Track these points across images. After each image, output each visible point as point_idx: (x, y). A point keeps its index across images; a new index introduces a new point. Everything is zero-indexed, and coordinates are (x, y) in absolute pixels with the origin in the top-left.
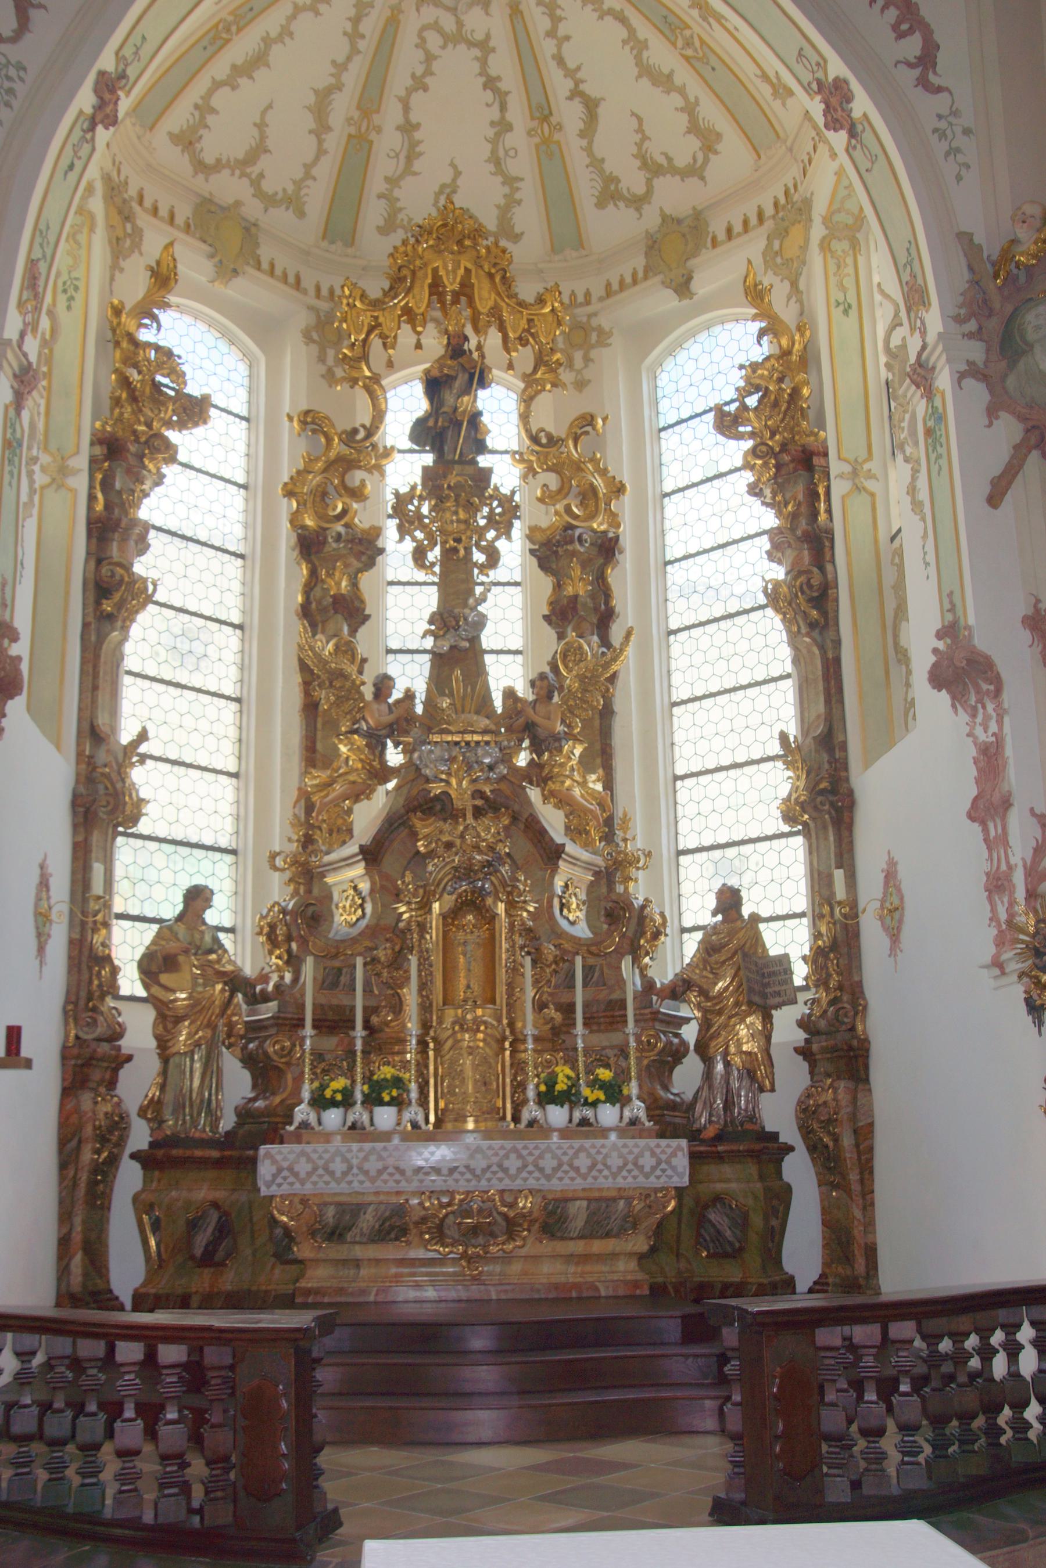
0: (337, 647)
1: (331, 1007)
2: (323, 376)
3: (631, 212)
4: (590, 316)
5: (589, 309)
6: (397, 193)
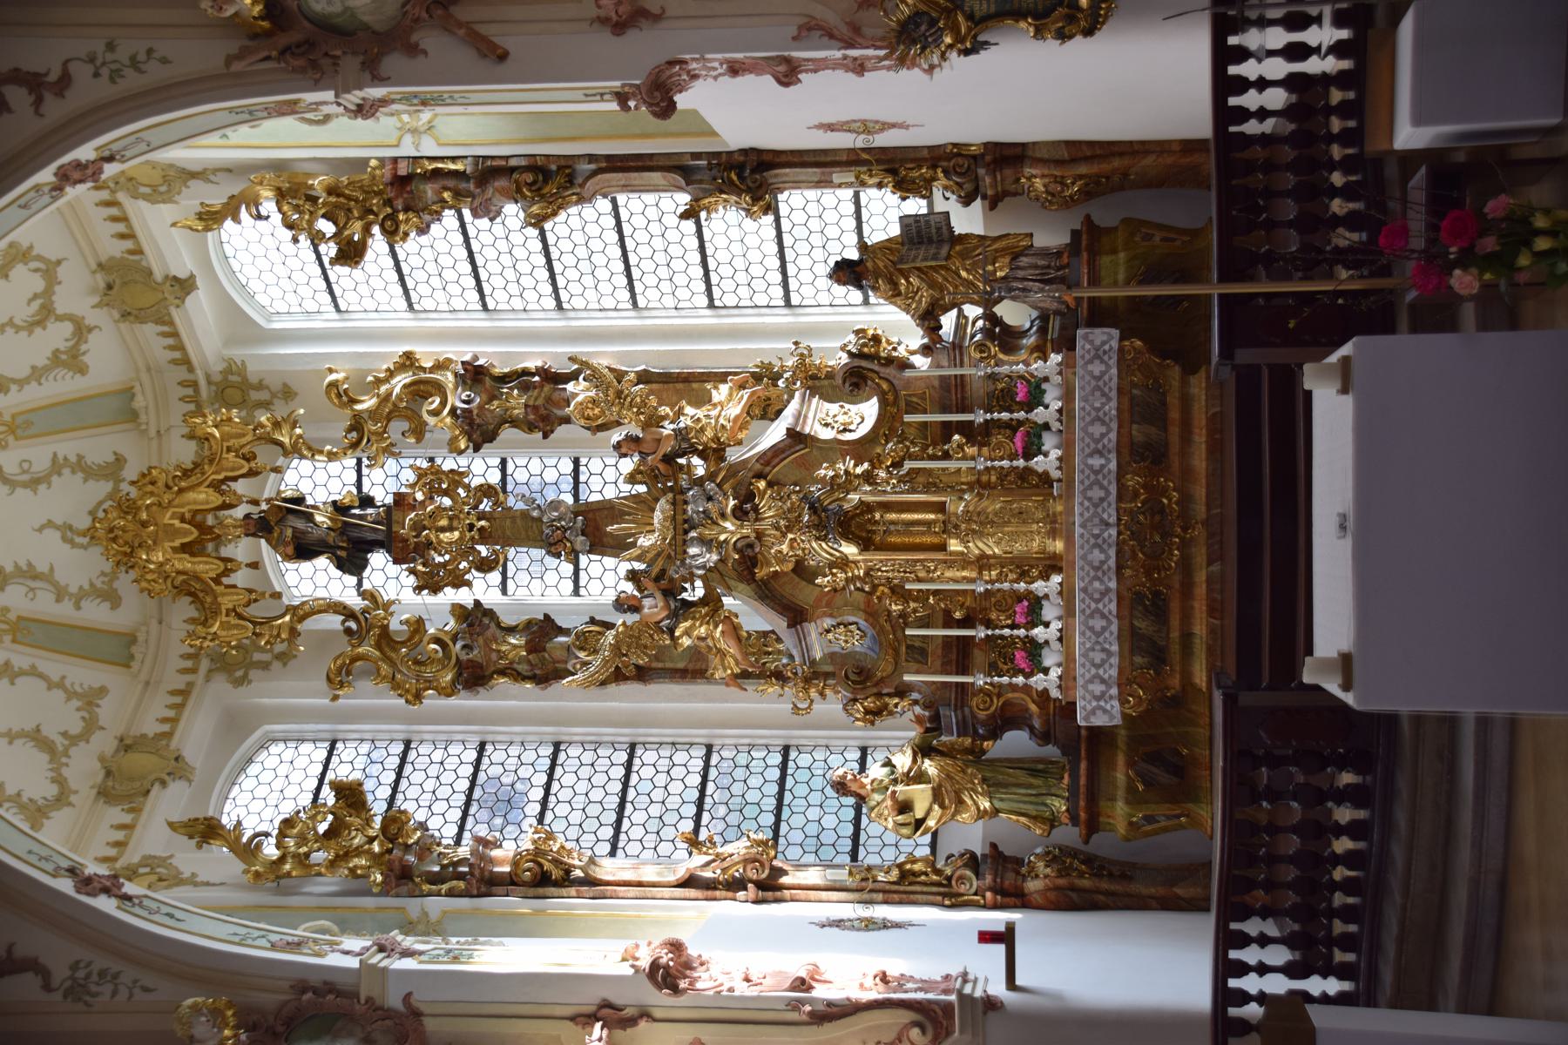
0: (582, 649)
1: (944, 656)
2: (285, 664)
3: (92, 337)
4: (209, 383)
5: (202, 383)
6: (73, 589)
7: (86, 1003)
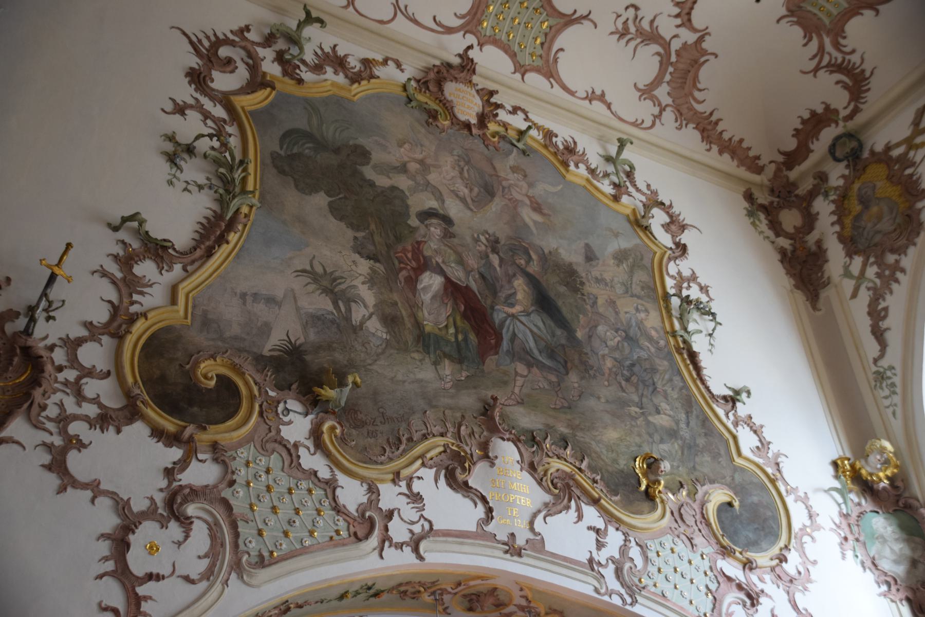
7: (876, 386)
